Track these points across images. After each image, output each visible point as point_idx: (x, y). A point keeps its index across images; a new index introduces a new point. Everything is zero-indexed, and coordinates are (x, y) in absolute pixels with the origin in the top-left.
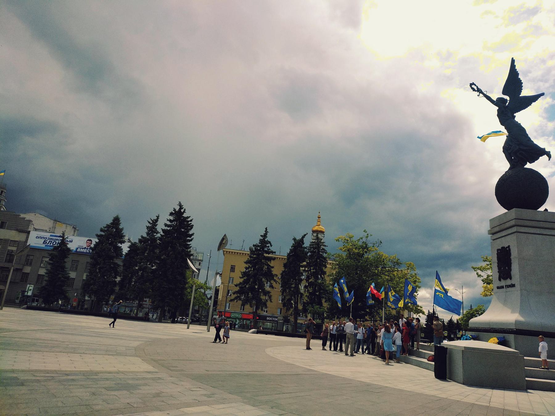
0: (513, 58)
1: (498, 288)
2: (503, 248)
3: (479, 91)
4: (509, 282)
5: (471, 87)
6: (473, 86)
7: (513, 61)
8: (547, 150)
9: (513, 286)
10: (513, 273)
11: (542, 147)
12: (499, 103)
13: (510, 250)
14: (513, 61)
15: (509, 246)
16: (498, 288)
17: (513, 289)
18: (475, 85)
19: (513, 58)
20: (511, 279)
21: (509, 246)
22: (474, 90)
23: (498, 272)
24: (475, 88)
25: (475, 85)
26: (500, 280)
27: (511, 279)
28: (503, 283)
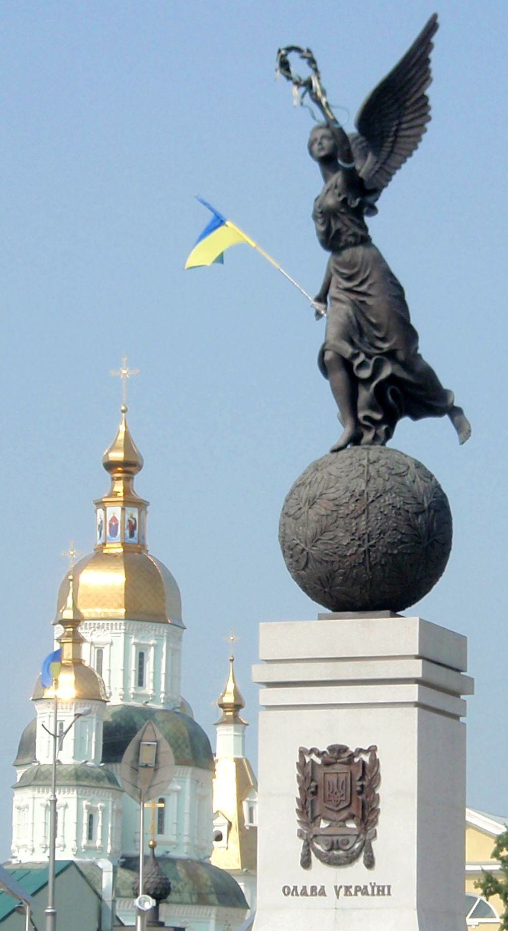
0: (435, 17)
1: (287, 891)
4: (356, 873)
6: (293, 57)
7: (432, 27)
9: (382, 891)
13: (375, 762)
14: (432, 27)
15: (372, 750)
16: (287, 891)
17: (377, 900)
18: (312, 61)
19: (435, 17)
21: (372, 750)
22: (285, 65)
25: (312, 61)
26: (306, 863)
28: (321, 874)
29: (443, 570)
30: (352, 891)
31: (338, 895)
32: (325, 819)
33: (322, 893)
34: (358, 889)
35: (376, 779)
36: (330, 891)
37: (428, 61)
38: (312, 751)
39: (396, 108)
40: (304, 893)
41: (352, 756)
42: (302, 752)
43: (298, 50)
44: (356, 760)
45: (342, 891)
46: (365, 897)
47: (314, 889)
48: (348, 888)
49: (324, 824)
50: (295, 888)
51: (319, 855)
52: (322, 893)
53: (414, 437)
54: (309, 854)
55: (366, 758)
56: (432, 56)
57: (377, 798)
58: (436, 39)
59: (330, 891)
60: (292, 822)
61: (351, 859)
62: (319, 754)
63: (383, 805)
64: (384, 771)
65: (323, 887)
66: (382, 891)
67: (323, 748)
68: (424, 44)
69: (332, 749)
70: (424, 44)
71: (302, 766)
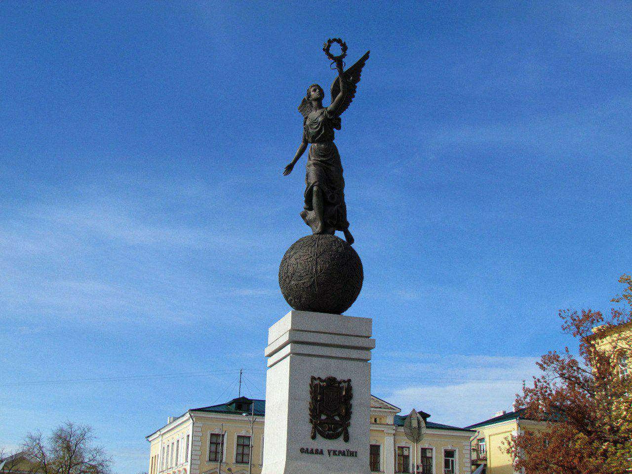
0: (369, 53)
1: (303, 451)
2: (332, 381)
3: (339, 61)
4: (339, 444)
5: (330, 42)
7: (366, 57)
8: (350, 229)
9: (353, 454)
10: (351, 430)
11: (349, 218)
13: (349, 389)
14: (366, 57)
15: (349, 381)
16: (303, 451)
17: (349, 459)
19: (369, 53)
20: (347, 439)
21: (349, 381)
22: (327, 50)
23: (311, 421)
25: (345, 48)
26: (314, 437)
27: (347, 439)
28: (322, 443)
29: (355, 299)
30: (337, 453)
32: (325, 414)
34: (340, 452)
36: (326, 452)
37: (361, 71)
38: (319, 378)
40: (312, 452)
41: (340, 383)
42: (313, 378)
43: (339, 41)
46: (343, 457)
47: (317, 450)
49: (323, 417)
52: (321, 453)
54: (315, 433)
56: (363, 69)
58: (367, 62)
59: (326, 452)
65: (322, 450)
66: (353, 454)
67: (323, 377)
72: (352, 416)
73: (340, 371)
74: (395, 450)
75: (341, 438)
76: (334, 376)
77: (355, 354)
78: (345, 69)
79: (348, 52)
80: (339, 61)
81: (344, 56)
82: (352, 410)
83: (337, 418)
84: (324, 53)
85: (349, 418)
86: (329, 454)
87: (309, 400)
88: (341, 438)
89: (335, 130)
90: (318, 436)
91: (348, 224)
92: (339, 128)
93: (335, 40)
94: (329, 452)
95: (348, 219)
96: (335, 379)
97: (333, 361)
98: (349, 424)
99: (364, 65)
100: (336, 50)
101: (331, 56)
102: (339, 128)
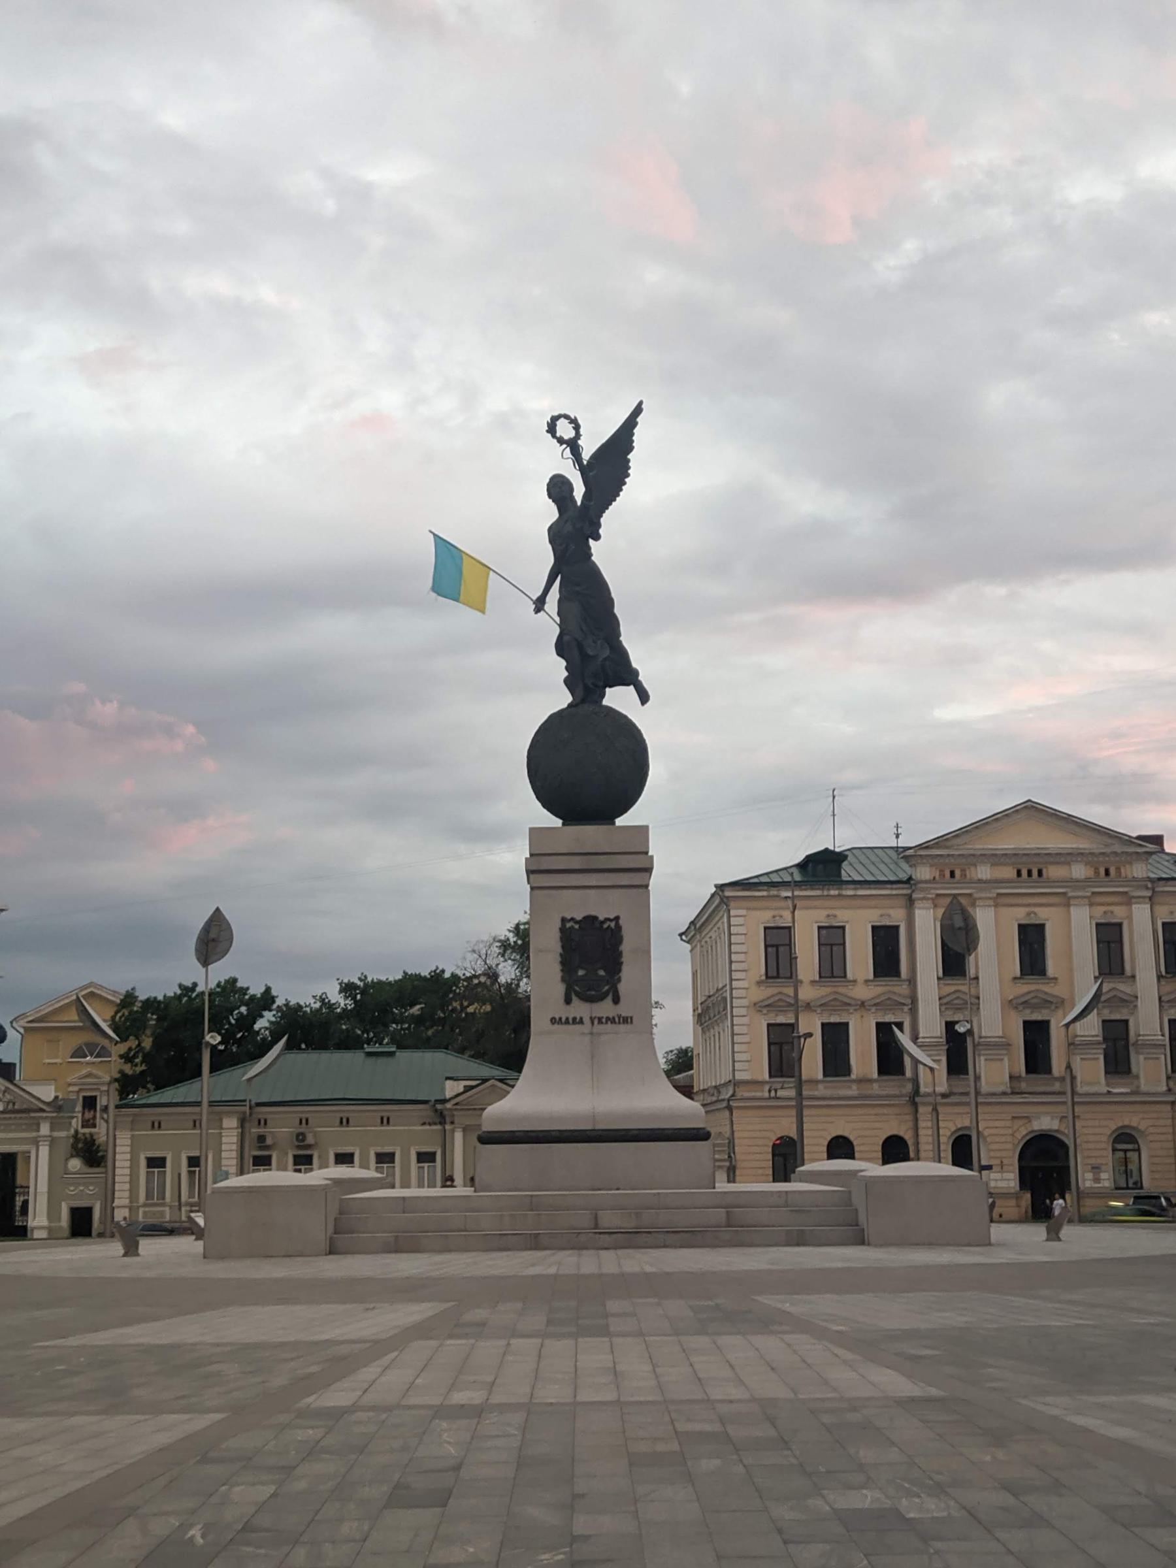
0: (641, 403)
1: (553, 1021)
3: (573, 445)
4: (605, 1008)
5: (554, 420)
7: (638, 410)
9: (626, 1020)
10: (622, 987)
12: (558, 489)
13: (619, 928)
14: (638, 410)
15: (617, 918)
16: (553, 1021)
17: (623, 1027)
19: (641, 403)
21: (617, 918)
22: (552, 429)
23: (563, 980)
24: (565, 430)
25: (577, 428)
26: (568, 1001)
27: (616, 1000)
28: (580, 1009)
31: (593, 1023)
32: (582, 968)
33: (581, 1022)
34: (608, 1019)
35: (620, 940)
36: (587, 1020)
37: (633, 434)
38: (572, 919)
39: (608, 468)
40: (567, 1022)
41: (603, 922)
42: (564, 920)
43: (566, 417)
44: (605, 926)
45: (596, 1022)
47: (574, 1019)
48: (600, 1019)
49: (581, 973)
50: (567, 1019)
51: (578, 995)
52: (581, 1022)
53: (618, 698)
55: (613, 925)
57: (620, 954)
59: (587, 1020)
60: (555, 971)
61: (601, 998)
62: (577, 922)
63: (625, 959)
64: (624, 932)
66: (626, 1020)
67: (579, 918)
68: (630, 424)
69: (586, 918)
70: (630, 424)
71: (562, 930)
72: (625, 968)
73: (602, 905)
74: (1155, 931)
75: (610, 998)
76: (593, 913)
77: (625, 879)
78: (586, 456)
79: (582, 431)
80: (573, 445)
81: (578, 435)
82: (623, 959)
83: (602, 973)
84: (549, 435)
85: (620, 971)
86: (593, 1023)
87: (560, 950)
88: (610, 998)
89: (591, 541)
90: (574, 997)
91: (636, 673)
92: (597, 537)
93: (559, 417)
94: (592, 1020)
95: (634, 665)
96: (595, 918)
97: (593, 892)
98: (619, 980)
99: (636, 424)
100: (565, 430)
101: (561, 441)
102: (597, 537)
